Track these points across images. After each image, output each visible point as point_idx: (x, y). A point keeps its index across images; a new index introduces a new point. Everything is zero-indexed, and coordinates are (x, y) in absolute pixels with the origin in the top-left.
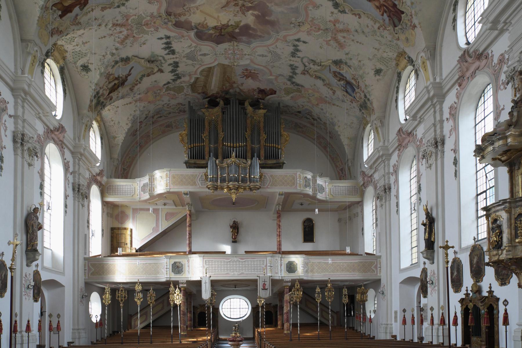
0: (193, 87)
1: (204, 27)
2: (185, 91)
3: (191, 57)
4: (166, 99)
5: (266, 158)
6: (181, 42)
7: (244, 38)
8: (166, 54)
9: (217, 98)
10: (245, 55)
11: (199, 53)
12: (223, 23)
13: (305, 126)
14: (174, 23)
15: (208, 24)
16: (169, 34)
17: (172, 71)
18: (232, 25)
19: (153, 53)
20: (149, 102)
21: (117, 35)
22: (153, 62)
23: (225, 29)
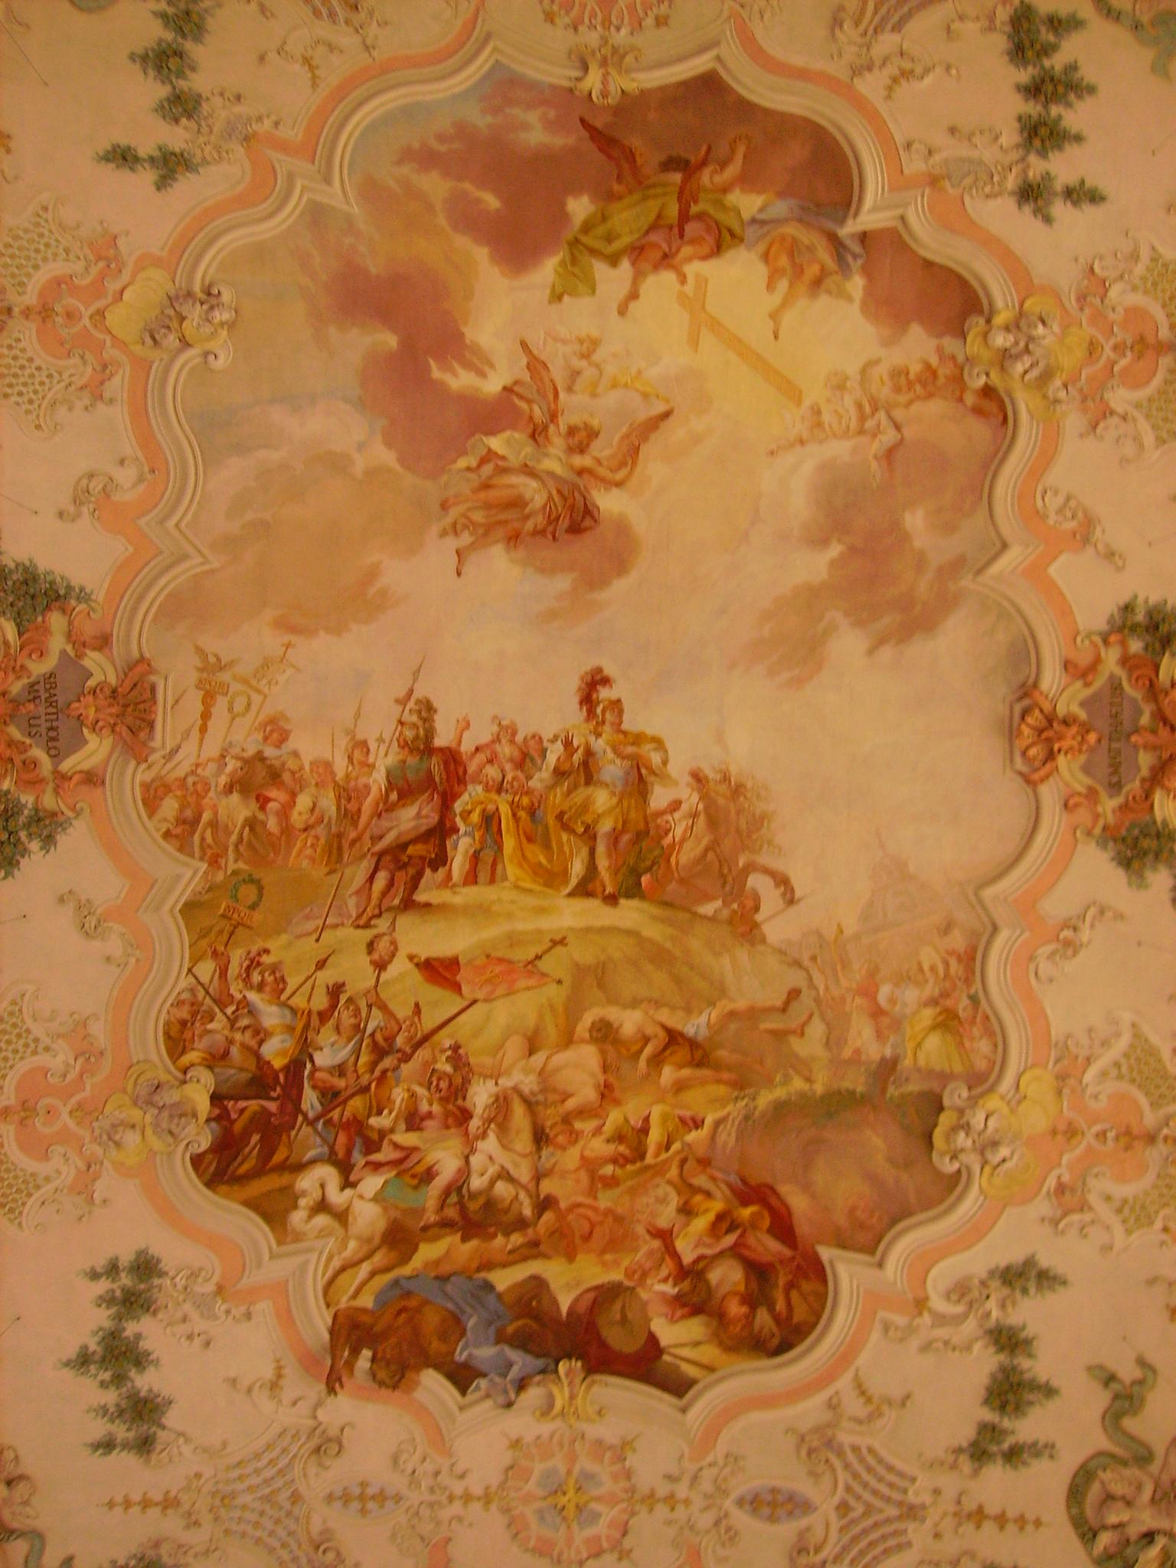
1: (793, 249)
6: (953, 130)
7: (536, 132)
12: (668, 277)
15: (761, 270)
18: (613, 261)
23: (654, 227)
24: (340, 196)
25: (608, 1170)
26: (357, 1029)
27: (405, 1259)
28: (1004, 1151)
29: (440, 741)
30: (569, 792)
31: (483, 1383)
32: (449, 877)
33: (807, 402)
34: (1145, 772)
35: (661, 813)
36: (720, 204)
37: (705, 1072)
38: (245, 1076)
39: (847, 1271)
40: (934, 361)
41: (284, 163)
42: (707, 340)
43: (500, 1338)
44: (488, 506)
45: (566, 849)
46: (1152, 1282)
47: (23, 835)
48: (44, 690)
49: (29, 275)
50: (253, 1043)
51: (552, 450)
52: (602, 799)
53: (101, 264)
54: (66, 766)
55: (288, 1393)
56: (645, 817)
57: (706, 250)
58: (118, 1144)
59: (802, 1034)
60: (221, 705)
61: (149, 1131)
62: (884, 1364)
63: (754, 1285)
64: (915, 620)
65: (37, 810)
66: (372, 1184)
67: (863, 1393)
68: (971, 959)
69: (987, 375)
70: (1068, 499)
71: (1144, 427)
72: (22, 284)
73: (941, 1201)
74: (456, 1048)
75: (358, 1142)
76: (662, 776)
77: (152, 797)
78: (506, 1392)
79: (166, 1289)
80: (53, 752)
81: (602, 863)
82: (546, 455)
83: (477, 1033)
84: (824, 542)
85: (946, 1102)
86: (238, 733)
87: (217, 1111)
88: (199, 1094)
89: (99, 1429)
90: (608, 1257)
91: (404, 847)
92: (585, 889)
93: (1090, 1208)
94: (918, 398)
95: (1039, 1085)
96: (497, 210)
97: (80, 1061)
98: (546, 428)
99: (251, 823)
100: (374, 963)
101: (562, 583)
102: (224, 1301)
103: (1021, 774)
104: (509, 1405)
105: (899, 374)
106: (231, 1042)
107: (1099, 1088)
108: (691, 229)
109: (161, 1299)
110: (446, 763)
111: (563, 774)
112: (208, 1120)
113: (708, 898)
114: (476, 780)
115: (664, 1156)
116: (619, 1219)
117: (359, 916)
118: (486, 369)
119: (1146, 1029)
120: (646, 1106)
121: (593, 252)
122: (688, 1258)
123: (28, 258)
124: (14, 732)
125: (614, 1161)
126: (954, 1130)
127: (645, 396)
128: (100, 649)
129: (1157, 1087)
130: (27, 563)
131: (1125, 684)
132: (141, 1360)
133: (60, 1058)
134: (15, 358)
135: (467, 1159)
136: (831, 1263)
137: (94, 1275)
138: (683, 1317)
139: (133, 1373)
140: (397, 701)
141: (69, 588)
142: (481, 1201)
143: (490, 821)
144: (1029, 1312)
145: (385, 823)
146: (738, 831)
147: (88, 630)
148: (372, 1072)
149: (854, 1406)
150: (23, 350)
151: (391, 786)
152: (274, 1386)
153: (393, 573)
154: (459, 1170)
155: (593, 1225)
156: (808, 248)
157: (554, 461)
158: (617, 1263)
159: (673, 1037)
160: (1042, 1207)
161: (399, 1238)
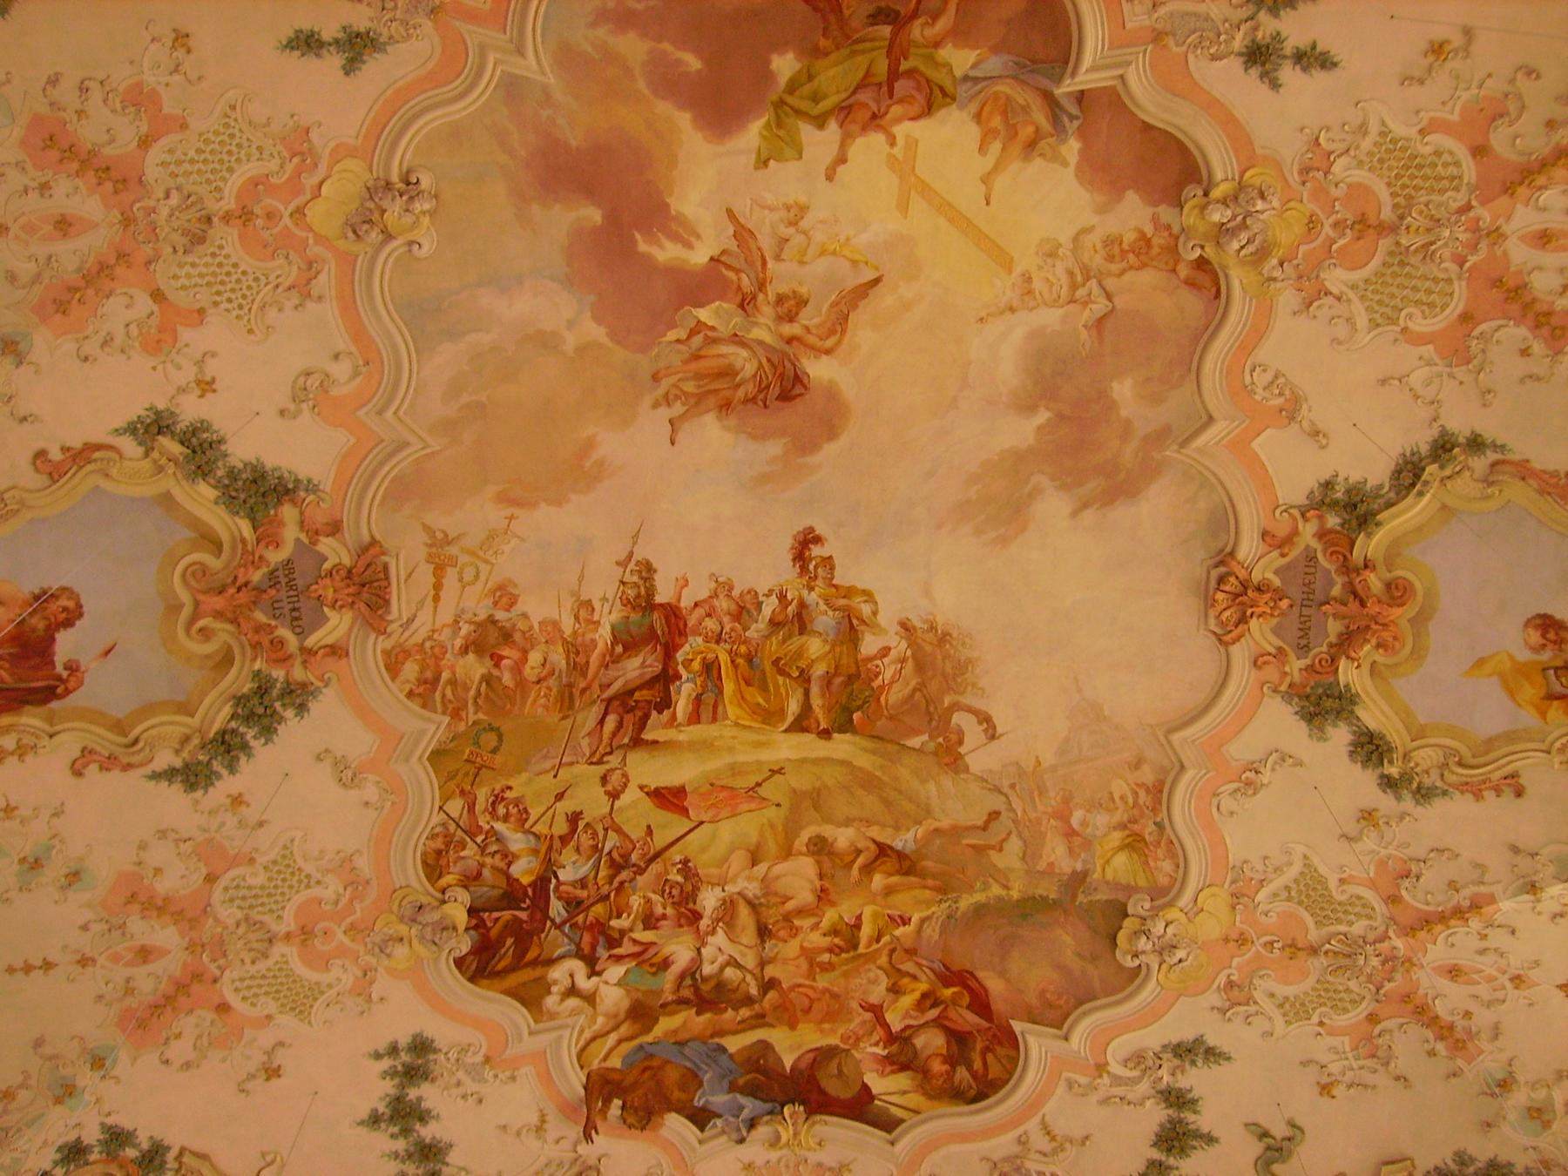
1: (1007, 108)
12: (877, 139)
14: (1193, 192)
15: (974, 131)
18: (820, 122)
23: (861, 86)
24: (536, 66)
25: (826, 957)
26: (596, 849)
28: (1181, 954)
29: (658, 599)
30: (784, 641)
31: (719, 1122)
33: (1018, 270)
34: (1333, 638)
35: (870, 659)
36: (931, 60)
37: (912, 879)
38: (496, 893)
39: (1037, 1043)
40: (1149, 230)
41: (474, 34)
42: (918, 205)
43: (733, 1088)
44: (698, 376)
45: (783, 690)
46: (1305, 1063)
47: (278, 705)
48: (283, 576)
49: (224, 179)
50: (503, 865)
51: (761, 320)
52: (815, 646)
53: (295, 160)
54: (311, 641)
55: (552, 1132)
56: (856, 662)
57: (915, 109)
58: (389, 956)
59: (1001, 850)
60: (451, 576)
61: (415, 942)
62: (1063, 1112)
63: (955, 1048)
64: (1120, 487)
65: (288, 684)
66: (615, 972)
68: (1159, 792)
69: (1202, 247)
70: (1276, 377)
71: (1358, 308)
72: (218, 189)
73: (1123, 989)
74: (685, 862)
75: (601, 939)
76: (872, 625)
77: (393, 664)
78: (739, 1130)
79: (440, 1063)
80: (298, 630)
81: (817, 702)
82: (756, 324)
83: (704, 850)
84: (1031, 409)
85: (1130, 911)
86: (467, 601)
87: (474, 922)
90: (826, 1026)
91: (631, 692)
92: (801, 725)
93: (1256, 1003)
94: (1131, 268)
95: (1216, 901)
96: (699, 71)
97: (349, 889)
98: (754, 297)
99: (487, 679)
100: (606, 793)
101: (774, 448)
102: (491, 1068)
104: (741, 1141)
105: (1113, 242)
106: (482, 865)
107: (1270, 906)
108: (901, 86)
109: (437, 1070)
110: (667, 618)
111: (778, 624)
112: (467, 929)
113: (918, 733)
114: (696, 633)
115: (875, 946)
116: (835, 996)
117: (593, 754)
118: (693, 239)
119: (1316, 861)
120: (861, 906)
121: (798, 113)
122: (896, 1027)
123: (221, 161)
124: (260, 617)
125: (830, 950)
126: (1136, 934)
127: (854, 263)
128: (331, 534)
129: (1322, 909)
130: (254, 462)
131: (1320, 555)
132: (423, 1117)
133: (331, 888)
134: (220, 265)
135: (699, 950)
137: (378, 1056)
138: (893, 1072)
139: (418, 1126)
140: (618, 563)
141: (297, 481)
142: (713, 983)
143: (710, 669)
144: (1195, 1079)
145: (612, 673)
146: (944, 675)
147: (320, 517)
148: (611, 883)
149: (1039, 1141)
150: (227, 257)
151: (616, 640)
152: (539, 1129)
153: (611, 445)
156: (1023, 107)
157: (763, 330)
158: (833, 1031)
159: (883, 850)
160: (1214, 998)
161: (641, 1013)
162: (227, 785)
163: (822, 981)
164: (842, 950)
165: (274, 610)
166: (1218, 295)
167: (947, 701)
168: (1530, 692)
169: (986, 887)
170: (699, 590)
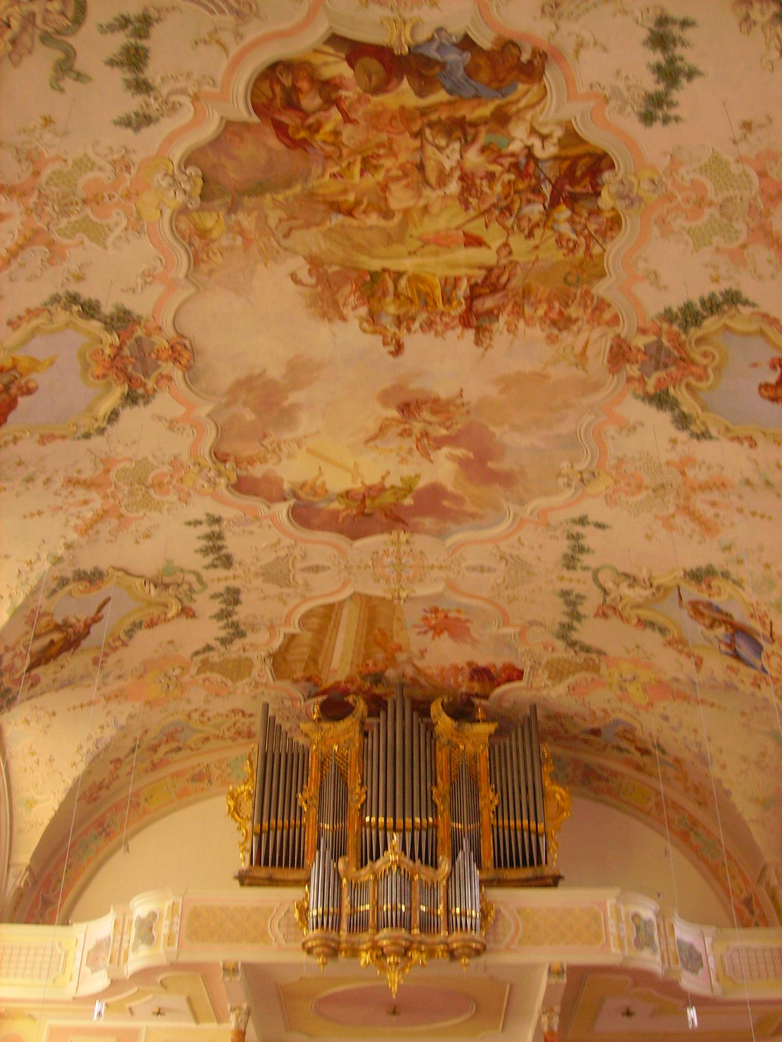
0: (278, 662)
2: (255, 672)
3: (277, 574)
4: (197, 696)
5: (498, 863)
6: (252, 533)
7: (428, 522)
8: (207, 567)
9: (346, 693)
10: (432, 567)
11: (300, 565)
12: (369, 482)
13: (615, 774)
14: (234, 480)
16: (217, 510)
17: (223, 615)
18: (393, 487)
19: (169, 562)
20: (148, 703)
21: (73, 510)
22: (167, 586)
25: (382, 152)
27: (499, 109)
31: (454, 40)
32: (468, 281)
37: (330, 199)
38: (582, 202)
39: (242, 112)
40: (249, 467)
43: (443, 65)
50: (575, 216)
59: (280, 220)
63: (294, 98)
64: (247, 384)
66: (515, 147)
67: (222, 45)
68: (196, 261)
75: (522, 168)
76: (362, 320)
77: (615, 320)
81: (390, 285)
88: (606, 200)
89: (688, 34)
90: (380, 108)
92: (398, 275)
99: (567, 305)
103: (186, 338)
107: (118, 219)
109: (641, 101)
110: (469, 322)
113: (336, 273)
114: (454, 318)
116: (375, 127)
125: (379, 156)
127: (377, 447)
131: (142, 377)
132: (658, 69)
133: (679, 223)
135: (462, 157)
136: (250, 113)
137: (677, 119)
139: (663, 62)
142: (454, 136)
143: (447, 300)
144: (133, 103)
146: (322, 300)
149: (227, 37)
152: (580, 45)
153: (492, 391)
154: (466, 151)
155: (390, 124)
157: (417, 427)
159: (350, 213)
160: (136, 158)
161: (502, 119)
162: (718, 289)
163: (384, 137)
164: (372, 157)
165: (669, 354)
166: (215, 455)
167: (319, 288)
168: (24, 364)
169: (286, 199)
170: (451, 335)
